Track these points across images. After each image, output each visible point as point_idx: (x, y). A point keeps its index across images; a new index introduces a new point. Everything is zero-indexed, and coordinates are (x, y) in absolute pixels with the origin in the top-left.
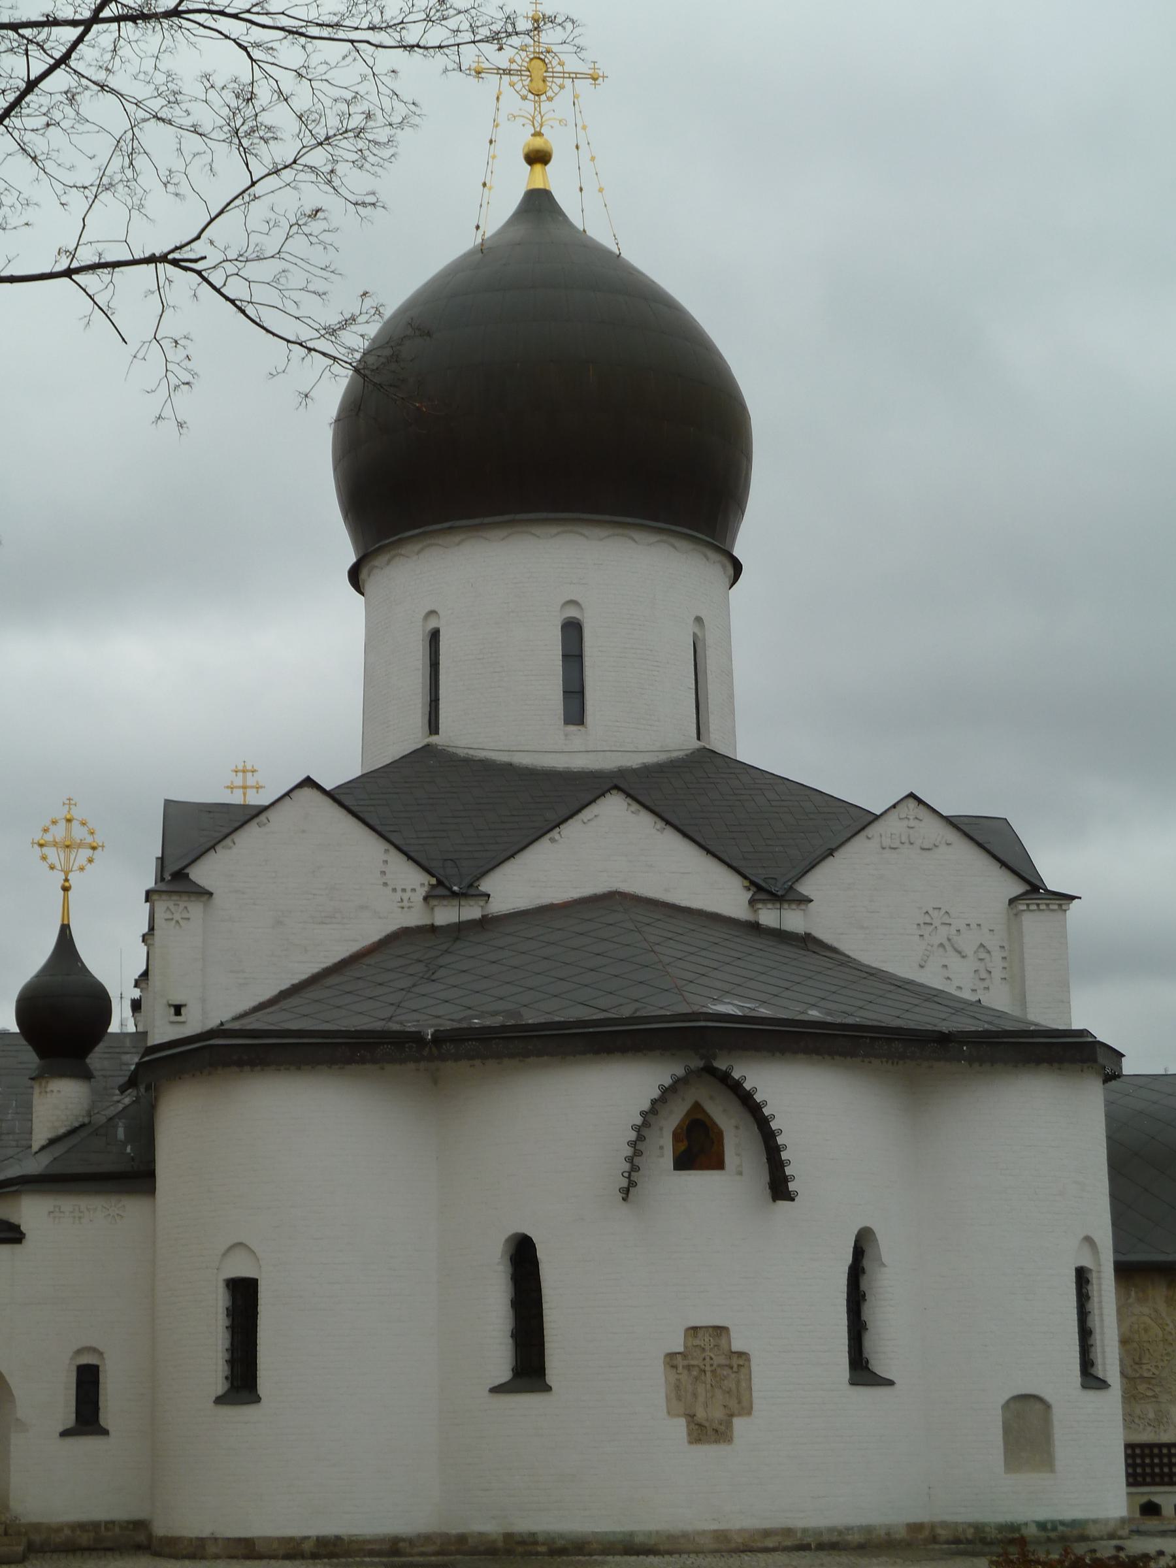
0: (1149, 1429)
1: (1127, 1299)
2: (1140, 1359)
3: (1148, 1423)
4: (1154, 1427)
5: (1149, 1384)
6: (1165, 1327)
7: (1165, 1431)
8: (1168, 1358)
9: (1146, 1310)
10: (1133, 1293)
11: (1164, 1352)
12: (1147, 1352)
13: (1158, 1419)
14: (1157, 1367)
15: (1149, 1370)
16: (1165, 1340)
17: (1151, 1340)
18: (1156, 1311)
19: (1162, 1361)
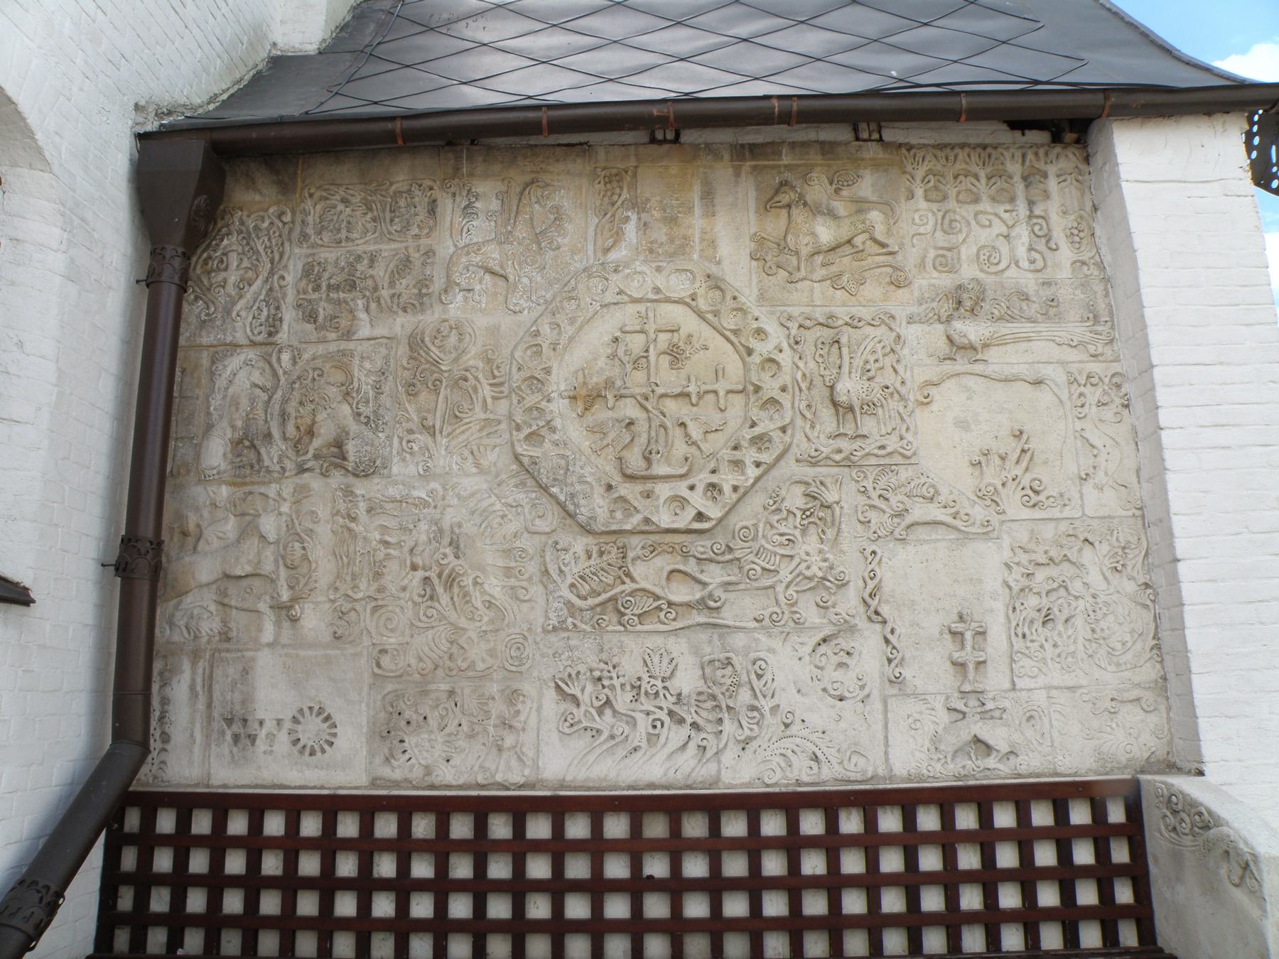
0: (675, 735)
1: (607, 251)
3: (671, 713)
4: (694, 725)
5: (686, 555)
6: (753, 343)
8: (766, 457)
9: (678, 285)
11: (748, 434)
12: (678, 432)
13: (714, 697)
14: (713, 489)
15: (682, 502)
17: (692, 389)
18: (716, 283)
19: (738, 464)
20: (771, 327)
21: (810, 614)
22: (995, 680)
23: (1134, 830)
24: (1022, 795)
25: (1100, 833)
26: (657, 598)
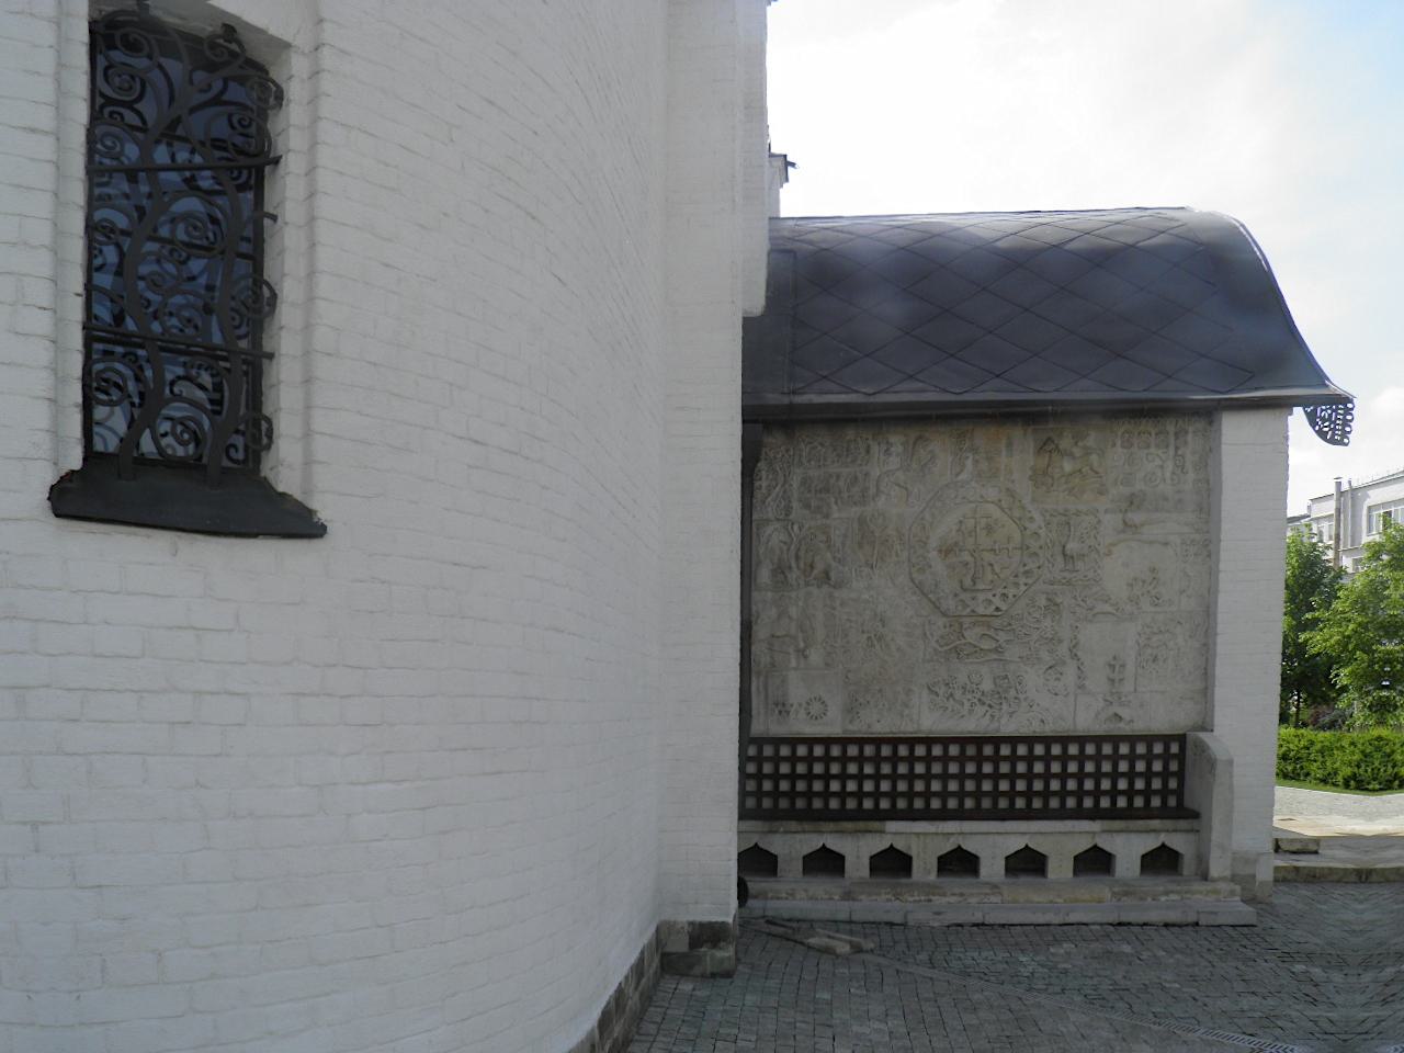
0: (980, 710)
1: (957, 475)
2: (974, 581)
3: (979, 700)
4: (990, 706)
5: (989, 627)
6: (1027, 524)
7: (1011, 714)
8: (1030, 581)
9: (992, 493)
10: (969, 463)
11: (1022, 570)
12: (989, 568)
13: (998, 693)
16: (1024, 547)
18: (1011, 493)
19: (1017, 585)
20: (1036, 515)
21: (1045, 655)
22: (1128, 687)
23: (1181, 757)
24: (1132, 740)
25: (1166, 757)
26: (975, 647)
